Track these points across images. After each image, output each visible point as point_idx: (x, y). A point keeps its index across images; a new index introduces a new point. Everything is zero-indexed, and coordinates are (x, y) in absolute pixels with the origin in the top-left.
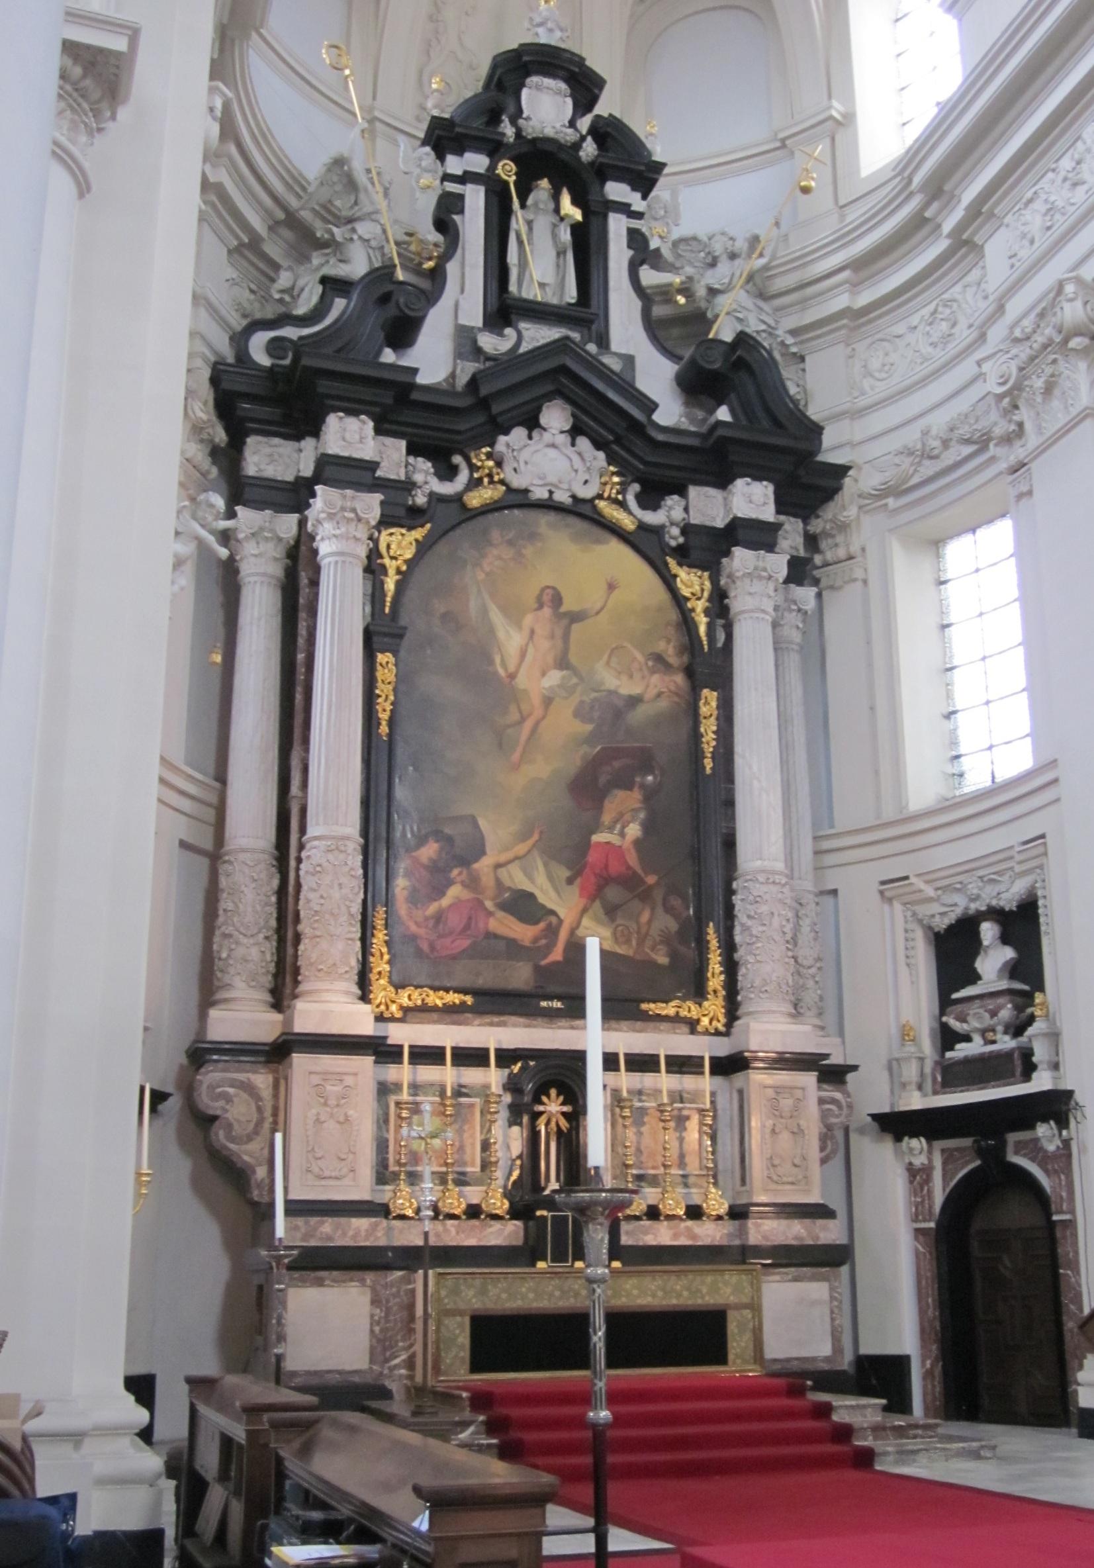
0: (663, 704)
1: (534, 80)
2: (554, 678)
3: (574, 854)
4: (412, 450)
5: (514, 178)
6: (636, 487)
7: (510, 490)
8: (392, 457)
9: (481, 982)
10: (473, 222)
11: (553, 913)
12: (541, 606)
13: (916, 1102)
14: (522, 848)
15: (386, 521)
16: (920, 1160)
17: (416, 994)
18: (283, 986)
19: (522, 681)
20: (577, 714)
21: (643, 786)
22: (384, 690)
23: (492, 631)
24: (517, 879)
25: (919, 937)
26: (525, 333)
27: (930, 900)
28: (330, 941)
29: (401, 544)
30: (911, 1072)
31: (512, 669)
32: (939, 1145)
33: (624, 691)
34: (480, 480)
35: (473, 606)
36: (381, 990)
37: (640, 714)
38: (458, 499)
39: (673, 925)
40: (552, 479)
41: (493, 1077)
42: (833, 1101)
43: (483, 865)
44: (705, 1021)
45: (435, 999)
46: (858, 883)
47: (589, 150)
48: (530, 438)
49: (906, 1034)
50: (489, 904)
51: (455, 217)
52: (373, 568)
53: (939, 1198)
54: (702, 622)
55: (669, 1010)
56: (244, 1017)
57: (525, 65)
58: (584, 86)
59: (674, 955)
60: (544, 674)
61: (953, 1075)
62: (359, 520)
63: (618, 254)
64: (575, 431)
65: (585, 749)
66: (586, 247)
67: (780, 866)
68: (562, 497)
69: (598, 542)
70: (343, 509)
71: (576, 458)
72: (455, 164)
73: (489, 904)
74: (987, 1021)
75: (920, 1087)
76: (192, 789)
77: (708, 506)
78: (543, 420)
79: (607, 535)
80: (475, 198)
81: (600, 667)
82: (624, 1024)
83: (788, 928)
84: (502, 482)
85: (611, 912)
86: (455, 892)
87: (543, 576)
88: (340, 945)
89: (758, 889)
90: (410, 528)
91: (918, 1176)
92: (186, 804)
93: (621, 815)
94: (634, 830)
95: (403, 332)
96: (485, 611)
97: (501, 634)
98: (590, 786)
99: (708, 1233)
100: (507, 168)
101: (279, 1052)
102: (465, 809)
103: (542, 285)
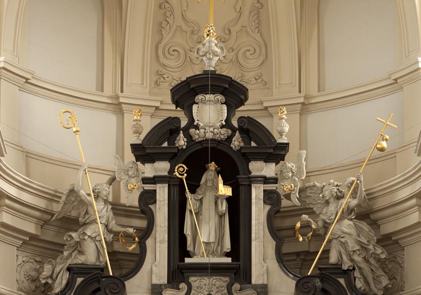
1: (199, 97)
5: (185, 175)
10: (161, 211)
47: (237, 142)
51: (150, 206)
57: (193, 89)
58: (233, 93)
63: (259, 212)
66: (237, 212)
72: (149, 170)
80: (162, 192)
100: (181, 169)
103: (207, 244)
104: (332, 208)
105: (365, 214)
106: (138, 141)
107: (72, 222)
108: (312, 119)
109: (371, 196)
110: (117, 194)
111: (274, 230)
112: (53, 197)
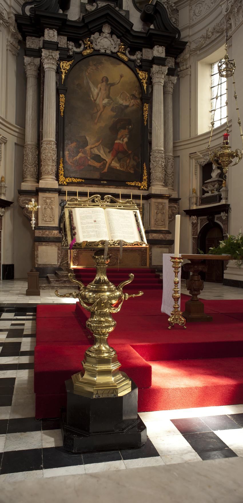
0: (134, 107)
2: (106, 101)
3: (110, 145)
4: (68, 40)
6: (129, 49)
7: (95, 50)
8: (63, 42)
9: (88, 176)
11: (105, 160)
12: (103, 82)
13: (194, 207)
14: (97, 144)
15: (61, 59)
16: (195, 221)
17: (70, 179)
18: (38, 177)
19: (98, 101)
20: (112, 110)
21: (128, 129)
22: (62, 104)
23: (90, 88)
24: (96, 151)
25: (198, 167)
26: (99, 5)
27: (201, 158)
28: (49, 166)
29: (66, 65)
30: (194, 200)
31: (95, 98)
32: (200, 218)
33: (124, 104)
34: (87, 47)
35: (85, 81)
36: (62, 178)
37: (129, 109)
38: (81, 53)
39: (135, 164)
40: (106, 47)
42: (174, 207)
43: (88, 148)
44: (142, 187)
46: (184, 155)
48: (100, 35)
49: (194, 191)
50: (89, 158)
52: (58, 72)
53: (199, 230)
54: (145, 86)
55: (133, 184)
56: (28, 185)
60: (103, 100)
61: (204, 201)
62: (54, 58)
64: (112, 33)
65: (114, 119)
67: (163, 149)
68: (108, 52)
69: (119, 64)
70: (49, 55)
71: (112, 41)
73: (89, 158)
74: (212, 188)
75: (196, 204)
76: (17, 130)
77: (148, 54)
78: (103, 30)
79: (120, 63)
81: (118, 98)
82: (122, 187)
83: (163, 164)
84: (92, 48)
85: (119, 160)
87: (104, 74)
88: (50, 167)
89: (156, 154)
90: (68, 61)
91: (194, 225)
92: (16, 134)
93: (122, 136)
94: (126, 140)
96: (88, 83)
97: (92, 89)
98: (115, 129)
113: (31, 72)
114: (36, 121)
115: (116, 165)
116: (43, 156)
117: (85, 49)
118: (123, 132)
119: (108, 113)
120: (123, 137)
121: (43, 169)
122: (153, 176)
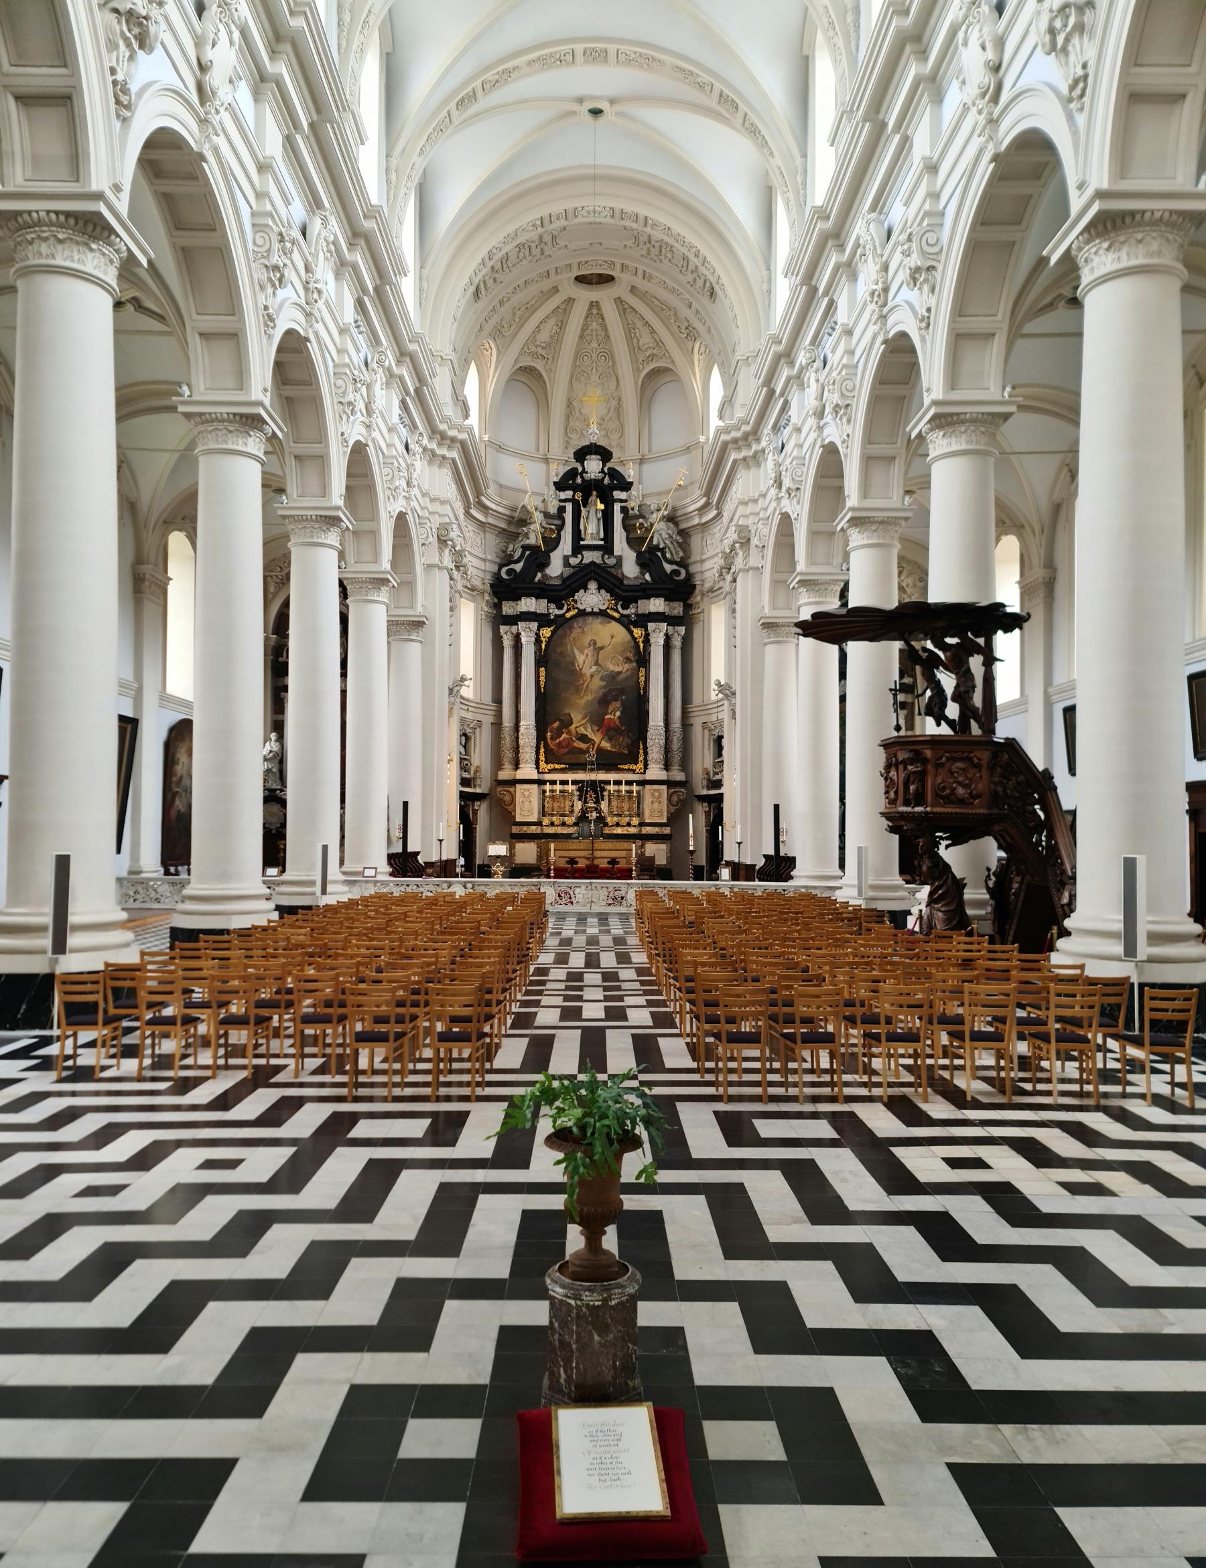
2: (594, 668)
3: (597, 720)
13: (705, 792)
15: (539, 629)
18: (516, 766)
20: (601, 679)
22: (542, 679)
24: (582, 731)
29: (546, 632)
30: (705, 783)
36: (542, 765)
37: (622, 676)
41: (570, 788)
45: (557, 766)
46: (697, 722)
47: (607, 481)
52: (538, 641)
54: (641, 645)
56: (505, 775)
58: (605, 455)
59: (630, 751)
63: (618, 517)
64: (599, 589)
66: (607, 517)
68: (596, 610)
80: (569, 507)
85: (610, 740)
86: (564, 736)
91: (707, 814)
94: (618, 714)
95: (544, 563)
98: (604, 701)
99: (633, 830)
101: (514, 782)
102: (567, 711)
104: (655, 515)
105: (671, 519)
106: (556, 480)
107: (524, 522)
108: (646, 468)
109: (674, 510)
110: (546, 506)
111: (626, 527)
112: (514, 509)
113: (507, 642)
114: (513, 699)
115: (606, 745)
116: (521, 742)
117: (568, 610)
118: (618, 704)
119: (597, 683)
120: (614, 711)
121: (521, 756)
122: (650, 758)
